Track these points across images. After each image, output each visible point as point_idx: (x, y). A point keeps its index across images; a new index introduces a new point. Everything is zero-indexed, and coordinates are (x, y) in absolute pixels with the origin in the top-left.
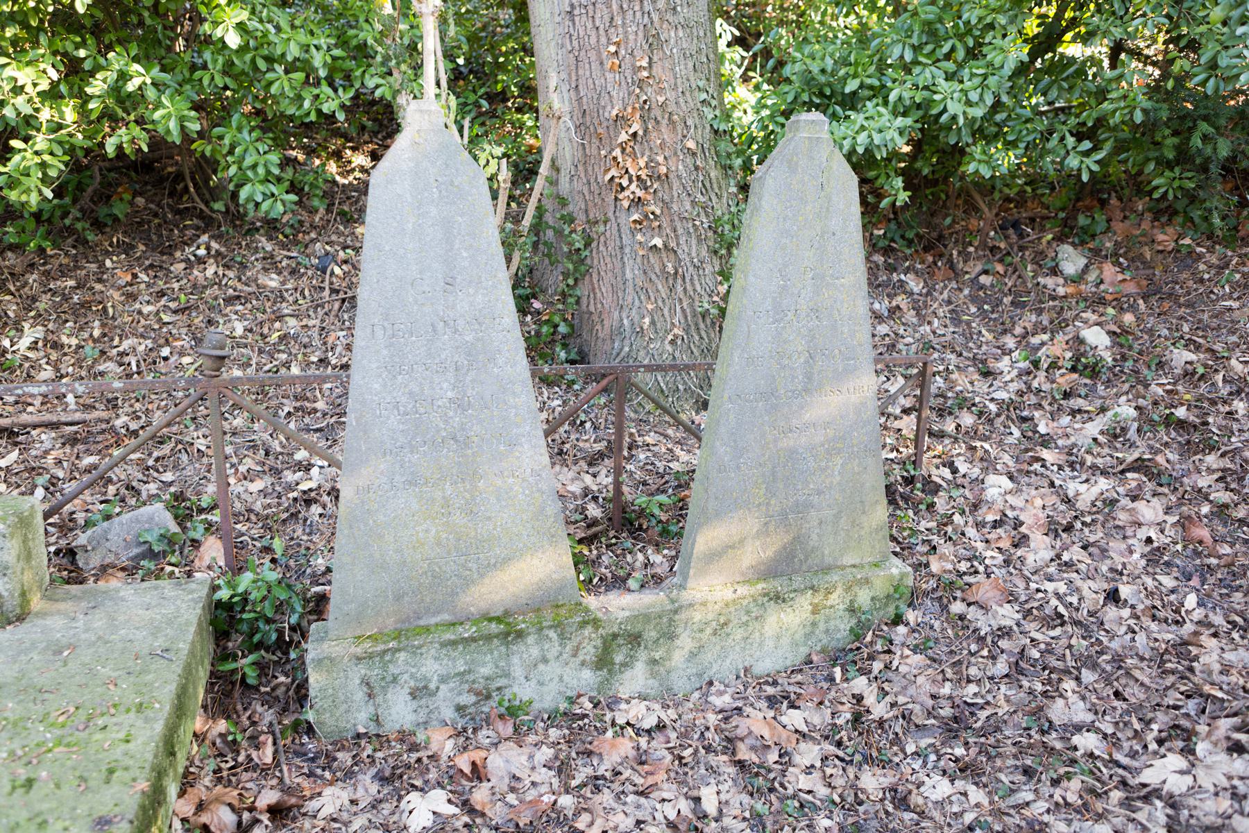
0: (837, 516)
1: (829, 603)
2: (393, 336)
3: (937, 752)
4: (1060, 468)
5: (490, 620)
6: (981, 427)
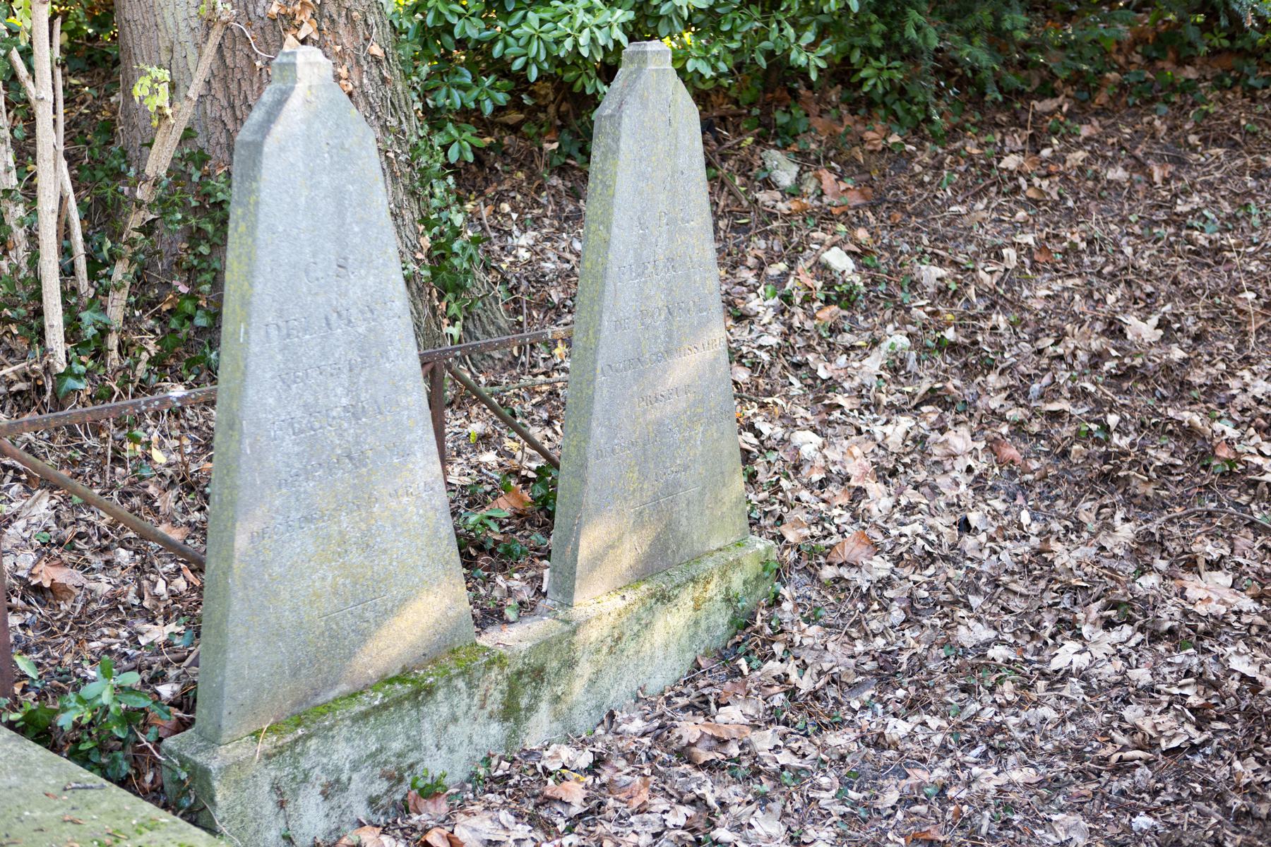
0: (702, 494)
1: (708, 595)
2: (288, 335)
3: (880, 700)
4: (861, 413)
5: (391, 681)
6: (761, 381)
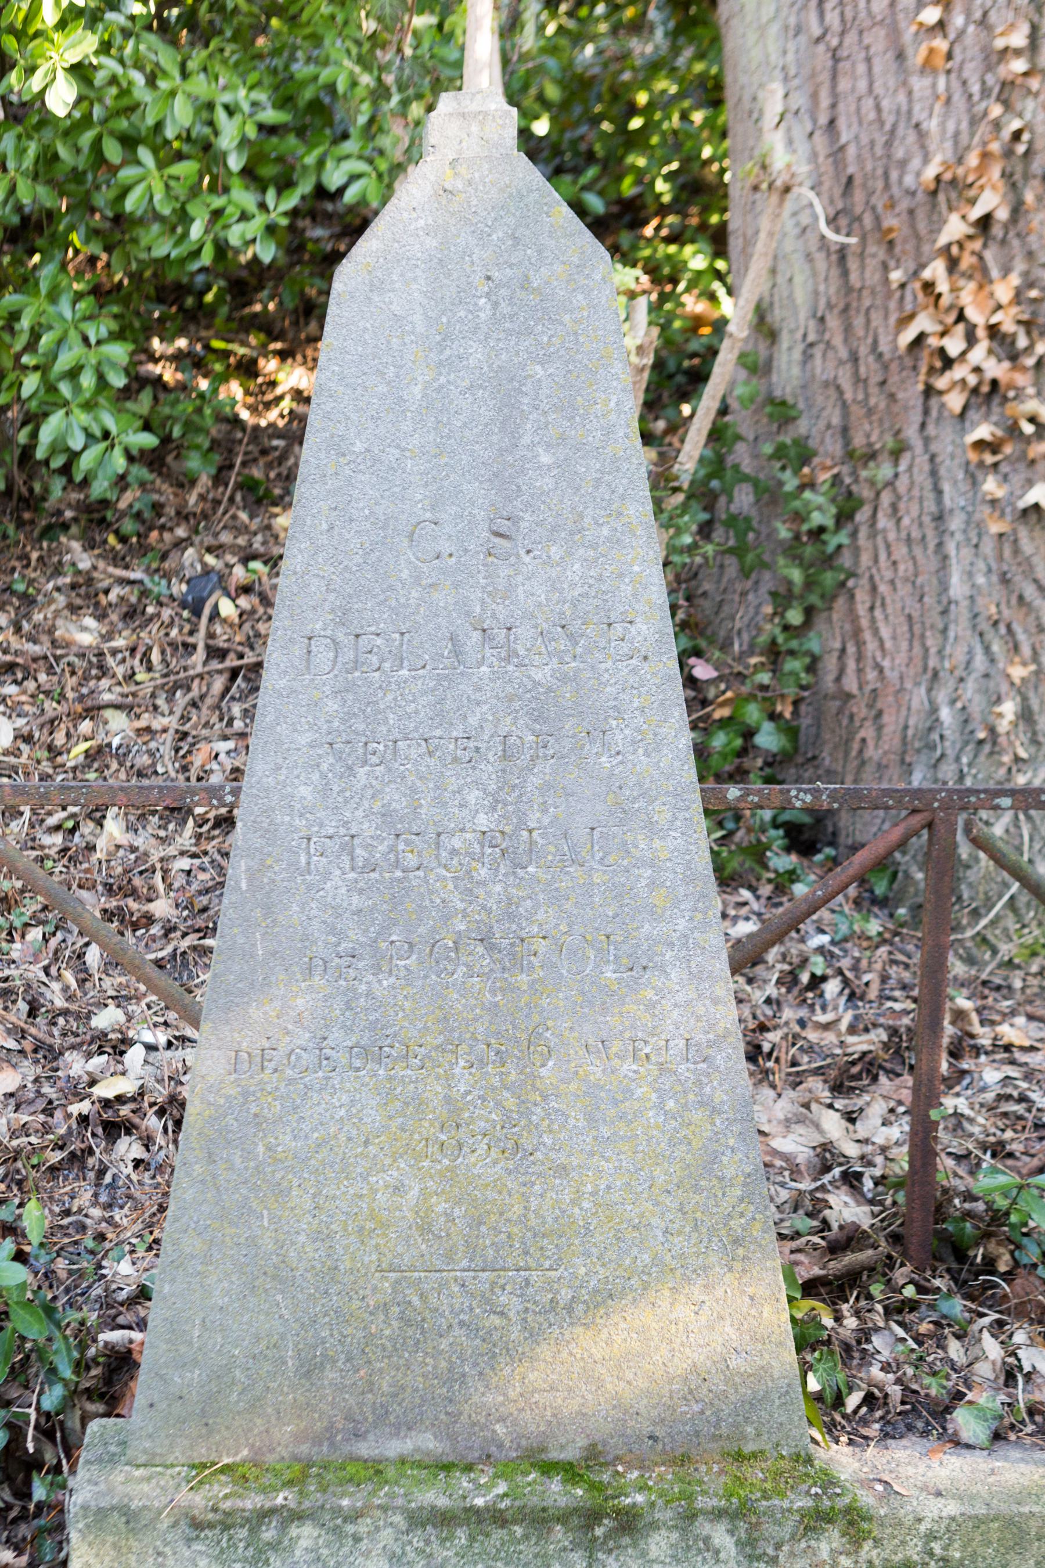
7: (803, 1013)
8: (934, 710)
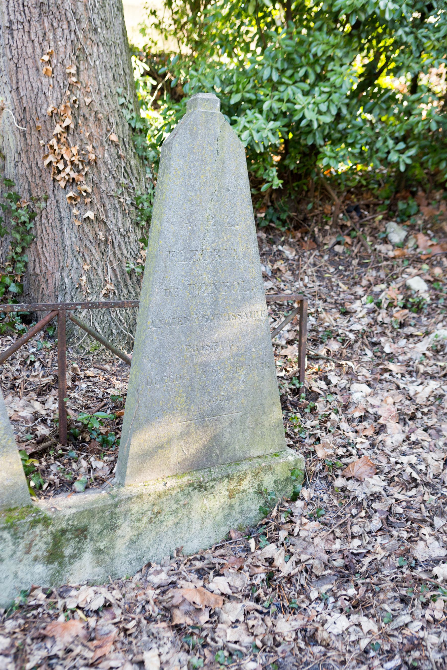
0: (244, 417)
1: (241, 488)
3: (334, 595)
4: (403, 376)
6: (344, 351)
7: (28, 373)
8: (63, 279)
